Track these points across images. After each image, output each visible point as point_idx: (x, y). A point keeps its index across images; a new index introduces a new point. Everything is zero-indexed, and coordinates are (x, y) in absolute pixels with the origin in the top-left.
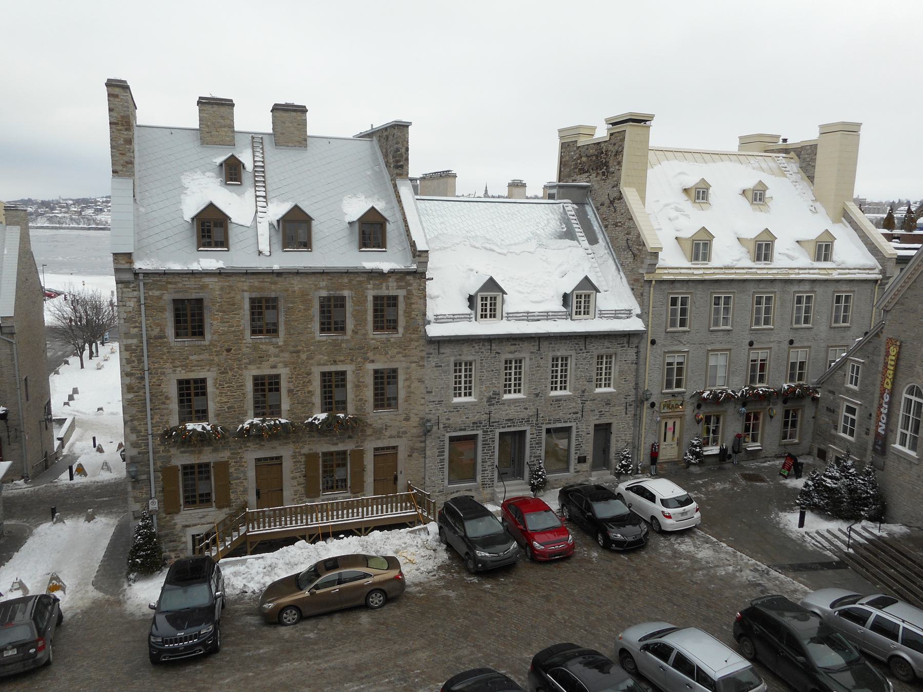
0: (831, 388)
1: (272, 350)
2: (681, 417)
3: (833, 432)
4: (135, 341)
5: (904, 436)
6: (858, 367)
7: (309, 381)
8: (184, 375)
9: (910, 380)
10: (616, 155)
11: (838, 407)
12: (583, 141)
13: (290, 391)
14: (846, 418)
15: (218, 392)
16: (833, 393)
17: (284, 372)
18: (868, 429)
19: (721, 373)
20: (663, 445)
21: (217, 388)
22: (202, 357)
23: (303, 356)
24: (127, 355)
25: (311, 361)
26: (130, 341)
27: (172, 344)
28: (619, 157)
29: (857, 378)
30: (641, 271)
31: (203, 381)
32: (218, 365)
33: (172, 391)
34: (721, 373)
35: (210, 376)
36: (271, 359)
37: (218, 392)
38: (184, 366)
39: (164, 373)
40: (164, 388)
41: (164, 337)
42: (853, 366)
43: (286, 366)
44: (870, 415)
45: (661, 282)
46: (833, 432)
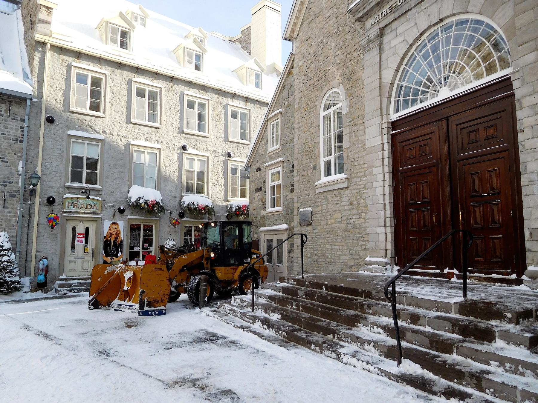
20: (69, 257)
44: (293, 166)
46: (263, 213)
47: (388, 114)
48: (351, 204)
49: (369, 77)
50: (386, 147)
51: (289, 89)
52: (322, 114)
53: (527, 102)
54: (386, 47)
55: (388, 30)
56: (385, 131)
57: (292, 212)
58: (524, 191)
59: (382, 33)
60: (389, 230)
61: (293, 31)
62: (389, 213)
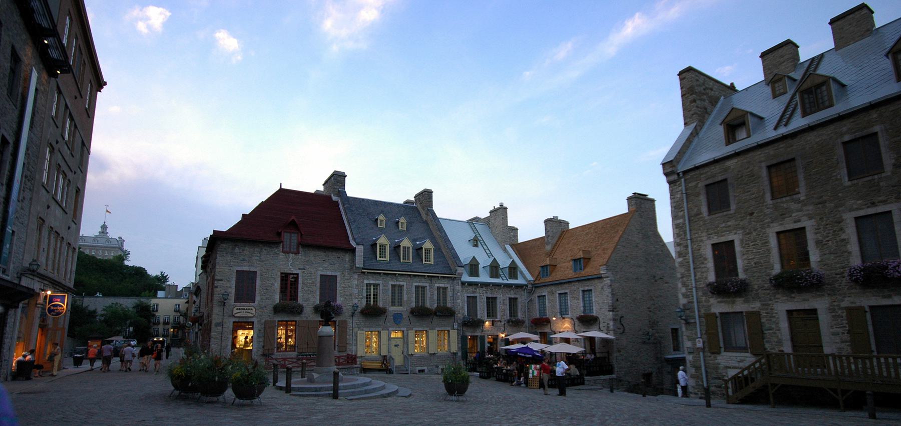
1: (793, 206)
4: (681, 221)
7: (841, 229)
8: (716, 240)
13: (818, 243)
15: (745, 250)
17: (808, 224)
21: (744, 247)
22: (729, 223)
23: (830, 205)
24: (677, 231)
25: (840, 209)
26: (678, 221)
27: (707, 218)
31: (732, 242)
32: (743, 228)
33: (708, 252)
35: (736, 238)
36: (794, 215)
37: (745, 250)
38: (717, 233)
39: (701, 241)
40: (702, 251)
41: (701, 214)
43: (810, 218)
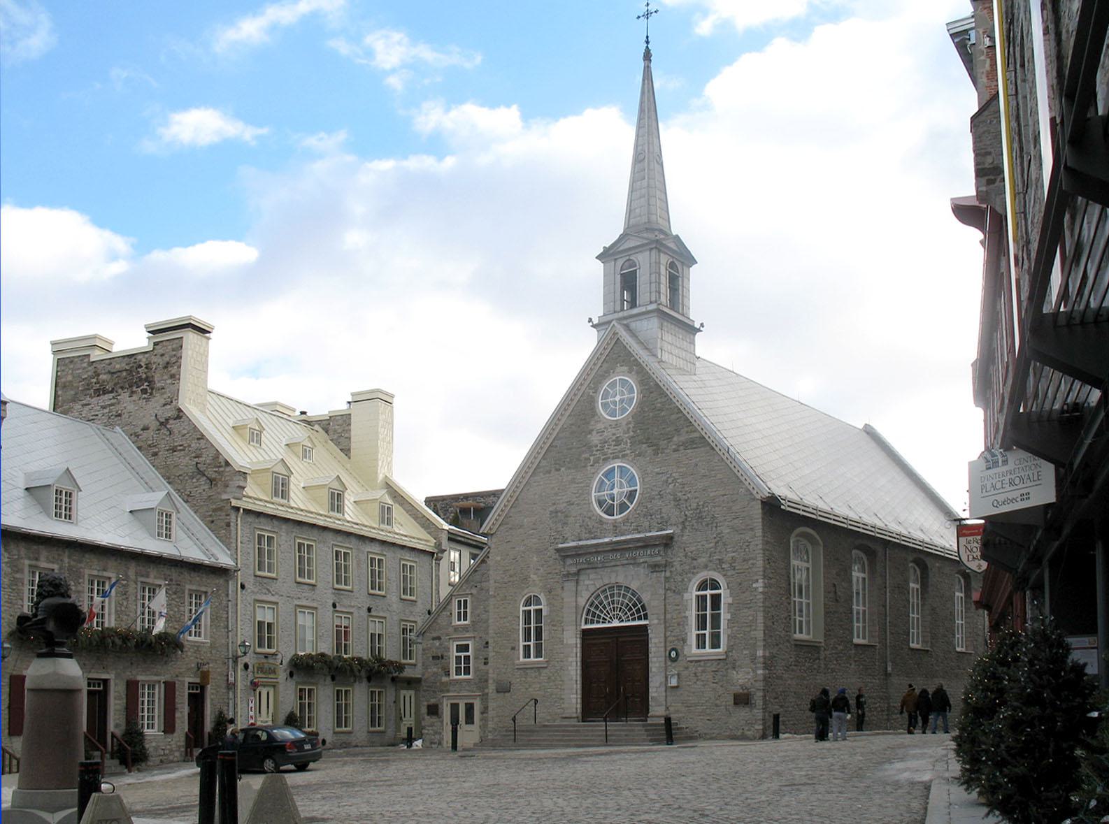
0: (435, 635)
2: (274, 686)
3: (445, 679)
5: (527, 648)
6: (465, 602)
9: (526, 591)
10: (166, 367)
11: (448, 649)
12: (96, 355)
14: (458, 658)
16: (439, 638)
18: (486, 659)
19: (309, 636)
28: (174, 370)
29: (465, 613)
30: (224, 497)
34: (309, 636)
42: (459, 602)
44: (487, 643)
45: (248, 512)
46: (445, 679)
47: (581, 625)
48: (549, 678)
49: (568, 598)
50: (579, 646)
51: (483, 574)
52: (522, 608)
53: (653, 641)
54: (581, 583)
55: (583, 572)
56: (578, 636)
57: (486, 681)
58: (650, 680)
59: (578, 573)
60: (579, 696)
61: (490, 529)
62: (579, 686)
